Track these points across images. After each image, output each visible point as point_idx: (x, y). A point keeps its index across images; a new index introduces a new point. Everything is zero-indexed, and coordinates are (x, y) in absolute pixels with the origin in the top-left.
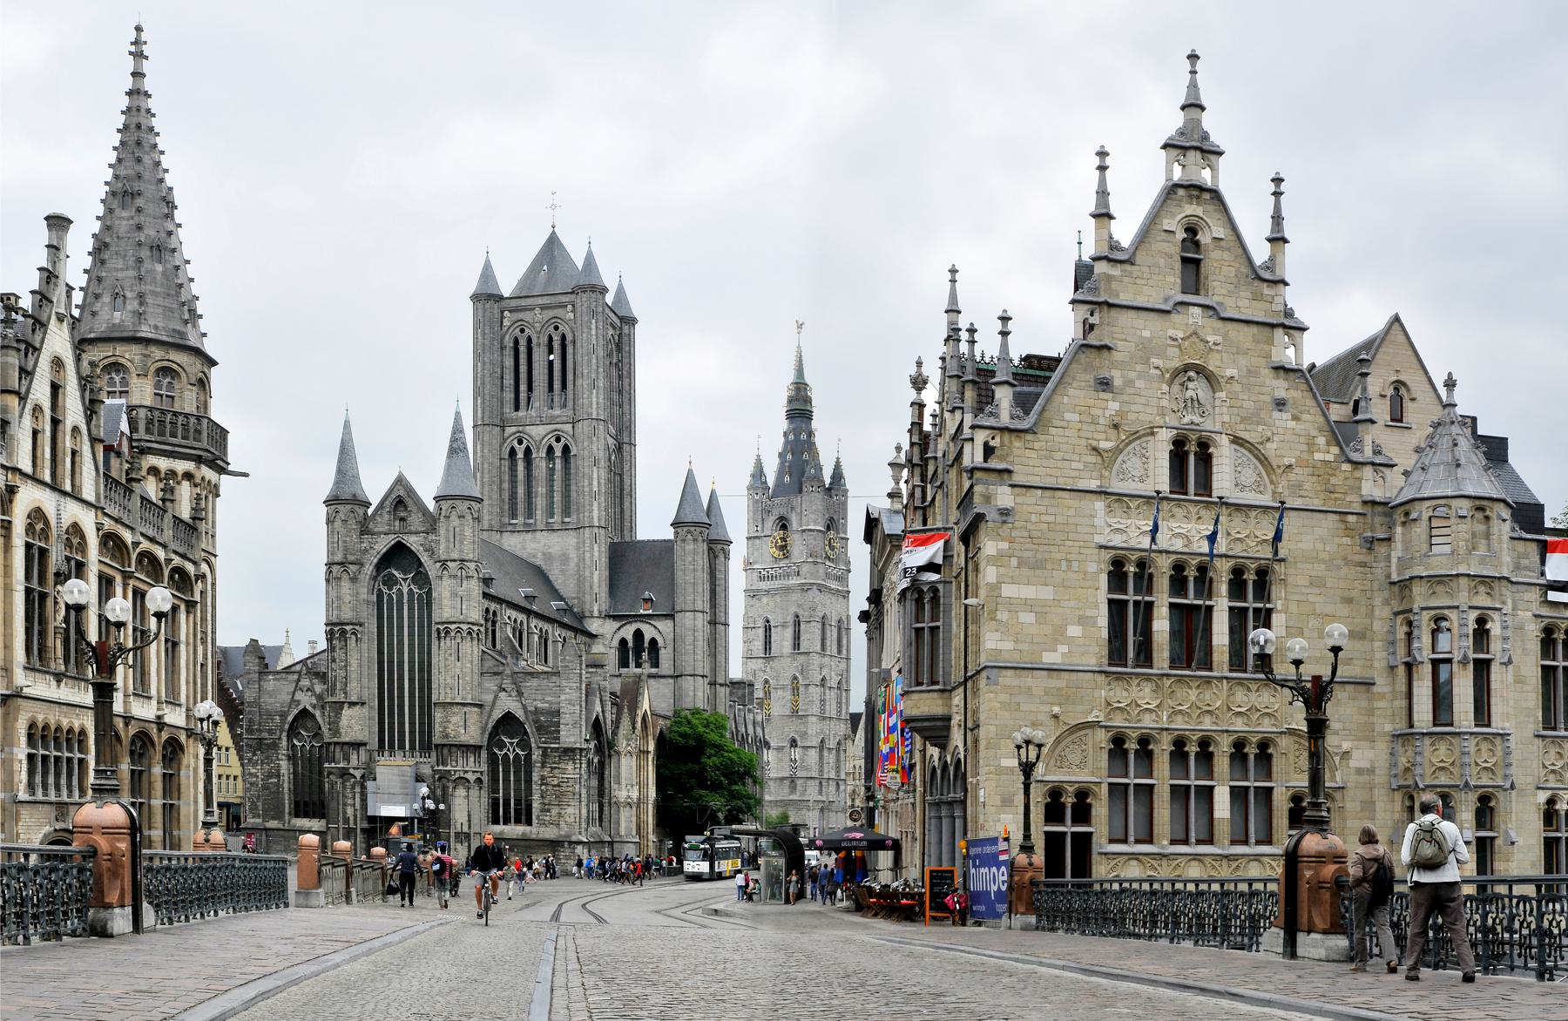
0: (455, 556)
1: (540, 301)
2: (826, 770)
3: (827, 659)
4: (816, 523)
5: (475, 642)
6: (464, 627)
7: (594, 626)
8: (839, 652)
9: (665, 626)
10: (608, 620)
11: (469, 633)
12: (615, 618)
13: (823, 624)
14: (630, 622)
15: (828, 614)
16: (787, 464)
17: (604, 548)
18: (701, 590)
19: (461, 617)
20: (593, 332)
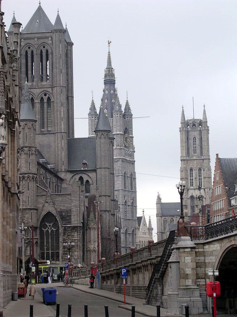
0: (27, 145)
1: (37, 35)
2: (128, 244)
3: (127, 192)
4: (120, 131)
5: (35, 182)
6: (31, 175)
7: (62, 175)
8: (132, 189)
9: (93, 175)
10: (68, 173)
11: (33, 178)
12: (71, 172)
13: (125, 176)
14: (78, 174)
15: (126, 171)
16: (105, 104)
17: (66, 142)
18: (107, 159)
19: (30, 171)
20: (61, 49)
